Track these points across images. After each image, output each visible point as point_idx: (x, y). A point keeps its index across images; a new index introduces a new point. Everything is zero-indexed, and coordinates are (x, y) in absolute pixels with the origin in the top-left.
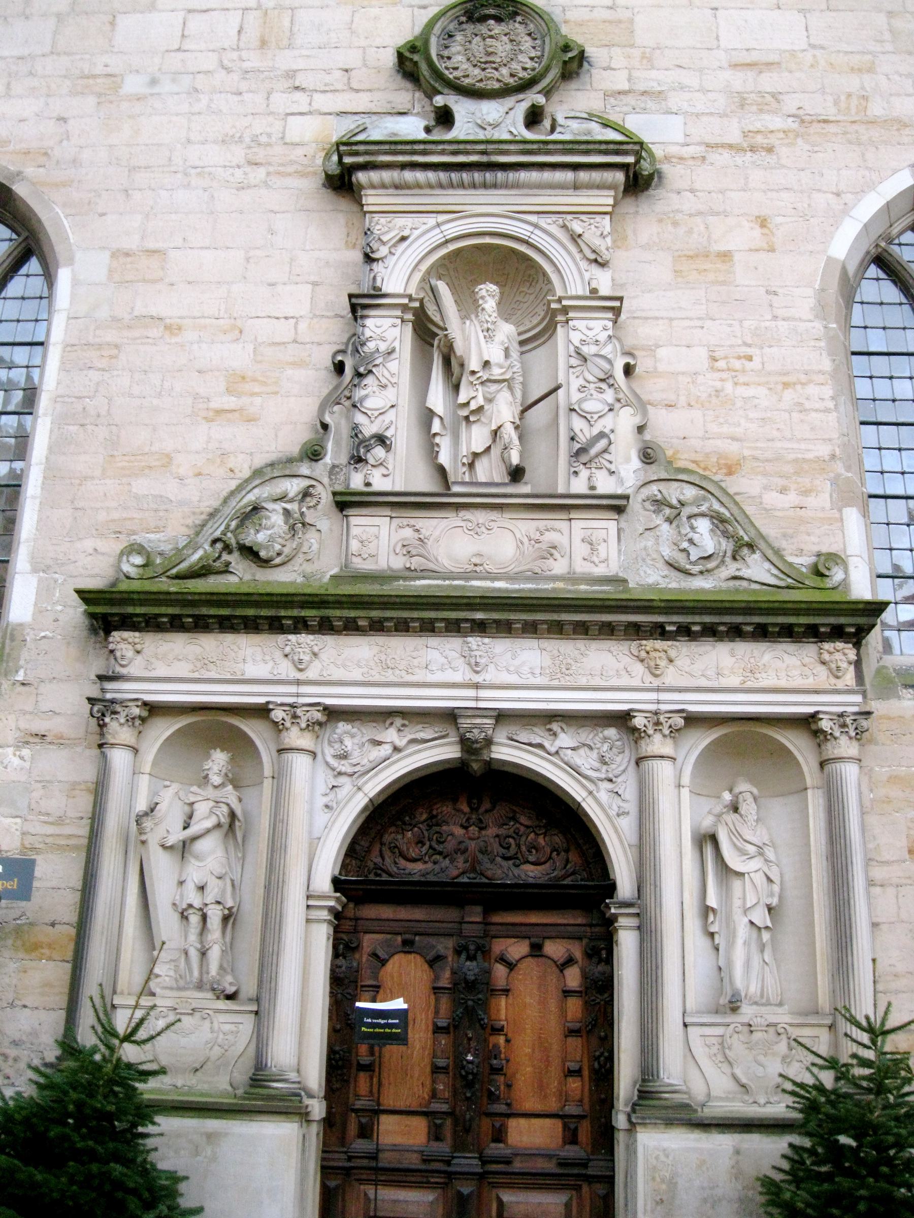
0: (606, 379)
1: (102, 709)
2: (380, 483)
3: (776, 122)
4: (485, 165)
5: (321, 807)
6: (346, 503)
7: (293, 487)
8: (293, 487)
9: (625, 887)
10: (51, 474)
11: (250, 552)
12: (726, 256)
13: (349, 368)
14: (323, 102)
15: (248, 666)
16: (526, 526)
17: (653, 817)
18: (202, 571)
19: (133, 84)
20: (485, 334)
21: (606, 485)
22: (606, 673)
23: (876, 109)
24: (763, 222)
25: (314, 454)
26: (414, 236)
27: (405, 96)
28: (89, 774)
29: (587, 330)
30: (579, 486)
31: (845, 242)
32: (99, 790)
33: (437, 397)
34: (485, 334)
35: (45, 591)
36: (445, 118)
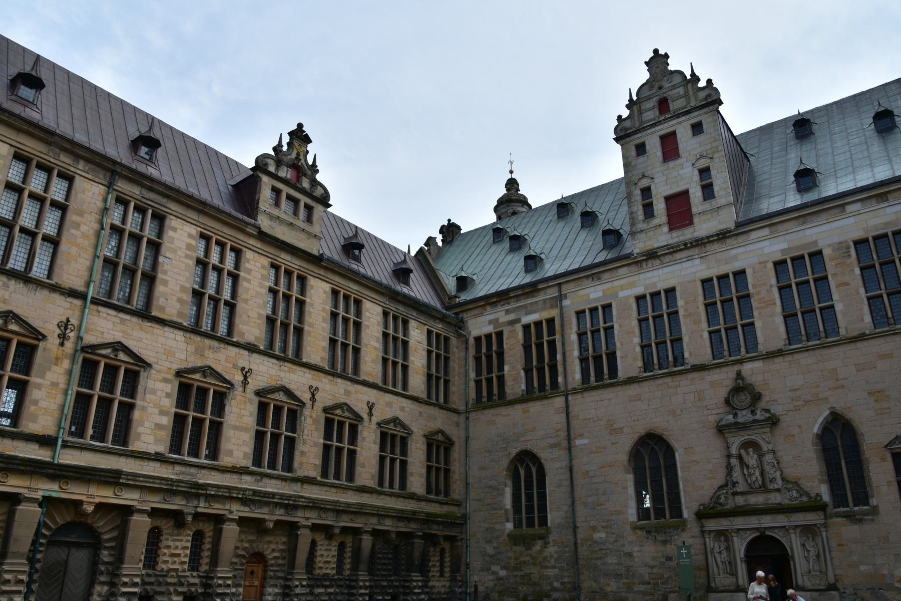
0: (774, 466)
1: (703, 532)
2: (739, 490)
3: (800, 403)
5: (740, 546)
6: (735, 494)
7: (724, 491)
8: (724, 491)
9: (790, 553)
10: (684, 492)
11: (720, 504)
12: (793, 435)
13: (729, 469)
14: (714, 412)
15: (724, 524)
16: (764, 495)
17: (794, 543)
18: (713, 507)
19: (678, 412)
20: (752, 459)
21: (776, 487)
22: (781, 520)
23: (821, 396)
24: (800, 427)
25: (726, 485)
26: (736, 441)
27: (728, 409)
28: (702, 542)
29: (769, 457)
30: (771, 487)
31: (816, 429)
32: (705, 544)
33: (746, 472)
34: (752, 459)
35: (689, 512)
36: (735, 415)
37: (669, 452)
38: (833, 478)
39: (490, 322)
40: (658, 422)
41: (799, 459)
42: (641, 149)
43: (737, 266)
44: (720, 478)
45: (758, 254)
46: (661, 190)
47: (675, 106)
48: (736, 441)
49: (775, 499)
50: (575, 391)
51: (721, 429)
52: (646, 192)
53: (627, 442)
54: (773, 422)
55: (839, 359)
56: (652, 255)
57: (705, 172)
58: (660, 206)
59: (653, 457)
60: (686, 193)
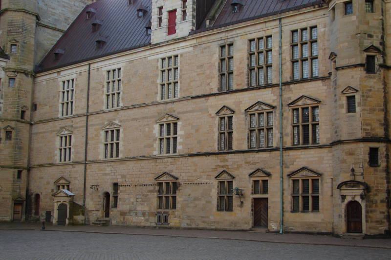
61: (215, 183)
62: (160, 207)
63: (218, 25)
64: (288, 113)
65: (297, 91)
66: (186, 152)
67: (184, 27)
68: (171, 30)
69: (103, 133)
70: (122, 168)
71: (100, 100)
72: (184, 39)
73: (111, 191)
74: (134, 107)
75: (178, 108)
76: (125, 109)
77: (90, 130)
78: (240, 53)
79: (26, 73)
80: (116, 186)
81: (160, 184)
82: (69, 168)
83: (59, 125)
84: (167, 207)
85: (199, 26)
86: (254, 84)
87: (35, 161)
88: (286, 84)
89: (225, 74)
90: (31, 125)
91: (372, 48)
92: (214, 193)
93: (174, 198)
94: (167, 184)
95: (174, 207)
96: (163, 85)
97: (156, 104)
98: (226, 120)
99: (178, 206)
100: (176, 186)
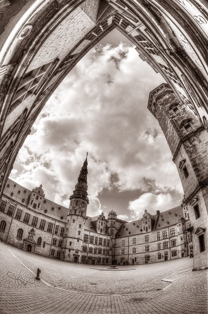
4: (32, 234)
13: (29, 237)
20: (31, 237)
22: (32, 244)
37: (23, 232)
38: (38, 242)
39: (6, 200)
40: (23, 228)
41: (35, 239)
42: (34, 195)
43: (38, 217)
44: (27, 237)
45: (41, 217)
46: (34, 202)
47: (40, 193)
48: (30, 235)
49: (32, 242)
50: (14, 218)
51: (29, 233)
52: (32, 201)
53: (18, 228)
54: (35, 235)
55: (43, 233)
56: (30, 209)
57: (39, 204)
58: (33, 204)
59: (21, 231)
60: (36, 205)
61: (158, 255)
62: (146, 260)
63: (156, 229)
64: (171, 242)
65: (171, 239)
66: (151, 251)
67: (149, 230)
68: (147, 231)
69: (132, 249)
70: (137, 255)
71: (131, 243)
72: (150, 232)
73: (134, 259)
74: (139, 244)
75: (149, 244)
76: (137, 245)
77: (129, 249)
78: (161, 234)
79: (114, 239)
80: (136, 258)
81: (146, 257)
82: (124, 256)
83: (121, 248)
84: (147, 260)
85: (152, 230)
86: (164, 238)
87: (116, 254)
88: (170, 238)
89: (158, 238)
90: (115, 248)
91: (184, 230)
92: (157, 257)
93: (149, 259)
94: (147, 257)
95: (149, 260)
96: (146, 240)
97: (145, 244)
98: (159, 245)
99: (150, 260)
100: (149, 257)
